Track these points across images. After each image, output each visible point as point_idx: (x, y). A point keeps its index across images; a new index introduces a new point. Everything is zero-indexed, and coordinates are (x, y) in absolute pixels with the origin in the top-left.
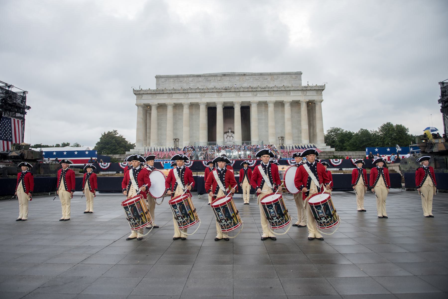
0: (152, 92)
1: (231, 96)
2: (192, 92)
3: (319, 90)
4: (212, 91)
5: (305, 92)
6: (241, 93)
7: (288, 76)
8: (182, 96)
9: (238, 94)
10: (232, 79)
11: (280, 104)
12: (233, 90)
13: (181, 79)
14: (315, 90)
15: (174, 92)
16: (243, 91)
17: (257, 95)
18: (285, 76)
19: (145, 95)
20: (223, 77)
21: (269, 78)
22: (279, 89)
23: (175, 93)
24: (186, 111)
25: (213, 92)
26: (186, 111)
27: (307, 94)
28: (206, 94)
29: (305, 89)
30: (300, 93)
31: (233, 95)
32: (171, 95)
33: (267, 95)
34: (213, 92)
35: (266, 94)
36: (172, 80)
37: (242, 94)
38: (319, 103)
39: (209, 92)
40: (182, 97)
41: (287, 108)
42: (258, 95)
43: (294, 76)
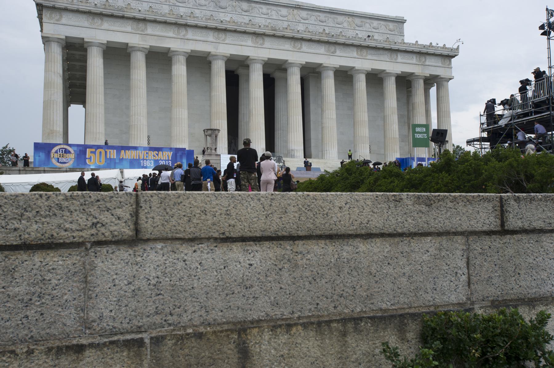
0: (93, 9)
2: (196, 27)
5: (423, 59)
7: (382, 23)
8: (170, 32)
9: (298, 44)
10: (274, 12)
12: (290, 34)
14: (441, 56)
16: (310, 40)
18: (375, 23)
19: (71, 15)
22: (380, 45)
23: (155, 21)
24: (180, 70)
25: (245, 33)
26: (180, 70)
27: (427, 63)
28: (228, 34)
29: (424, 50)
30: (414, 59)
31: (288, 45)
32: (141, 25)
34: (245, 33)
35: (354, 53)
37: (305, 47)
39: (235, 31)
40: (171, 34)
41: (391, 87)
43: (391, 25)
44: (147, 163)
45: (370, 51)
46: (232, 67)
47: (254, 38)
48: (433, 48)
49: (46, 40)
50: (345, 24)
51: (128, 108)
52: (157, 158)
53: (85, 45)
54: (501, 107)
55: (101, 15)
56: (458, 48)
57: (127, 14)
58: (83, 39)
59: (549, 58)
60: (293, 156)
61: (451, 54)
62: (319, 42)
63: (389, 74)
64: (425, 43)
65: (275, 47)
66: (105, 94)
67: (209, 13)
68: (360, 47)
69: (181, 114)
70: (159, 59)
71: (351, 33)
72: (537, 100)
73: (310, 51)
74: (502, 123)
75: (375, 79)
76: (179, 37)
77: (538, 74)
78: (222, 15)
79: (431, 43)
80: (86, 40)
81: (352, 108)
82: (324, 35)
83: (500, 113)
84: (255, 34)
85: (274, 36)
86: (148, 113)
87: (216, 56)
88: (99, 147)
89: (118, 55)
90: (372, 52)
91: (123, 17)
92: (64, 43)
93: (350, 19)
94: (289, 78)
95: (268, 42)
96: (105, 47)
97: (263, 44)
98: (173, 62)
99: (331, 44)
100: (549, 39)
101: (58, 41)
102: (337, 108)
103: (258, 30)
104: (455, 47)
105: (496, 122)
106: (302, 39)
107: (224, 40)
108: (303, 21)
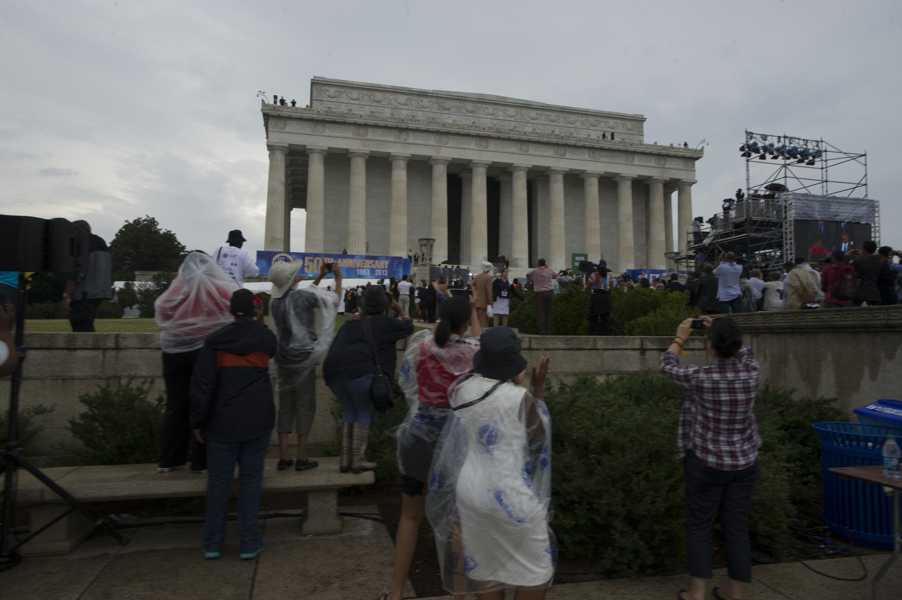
0: (316, 117)
1: (507, 150)
2: (417, 130)
4: (466, 131)
6: (531, 146)
7: (619, 121)
8: (391, 137)
10: (500, 113)
11: (609, 183)
12: (516, 137)
13: (379, 96)
14: (683, 158)
15: (373, 122)
17: (564, 154)
18: (612, 122)
19: (294, 123)
20: (478, 105)
21: (578, 120)
23: (376, 126)
24: (400, 175)
25: (468, 135)
26: (400, 175)
27: (668, 166)
28: (450, 137)
29: (664, 152)
30: (653, 162)
31: (513, 148)
32: (362, 130)
33: (587, 157)
34: (468, 135)
35: (586, 155)
36: (355, 94)
37: (532, 149)
38: (687, 188)
39: (458, 134)
40: (392, 139)
42: (568, 155)
43: (629, 125)
44: (363, 272)
45: (603, 153)
47: (478, 140)
49: (270, 147)
50: (578, 124)
51: (347, 214)
52: (373, 267)
53: (307, 152)
54: (709, 225)
55: (323, 122)
57: (349, 120)
58: (305, 146)
59: (748, 180)
60: (516, 266)
61: (695, 156)
62: (547, 144)
63: (624, 178)
64: (664, 144)
65: (500, 150)
66: (326, 201)
67: (431, 115)
68: (592, 149)
69: (400, 221)
70: (379, 165)
71: (583, 134)
72: (737, 221)
73: (537, 153)
74: (706, 241)
77: (739, 195)
78: (445, 116)
81: (583, 214)
83: (708, 230)
84: (478, 136)
85: (498, 138)
86: (367, 219)
87: (437, 161)
88: (316, 255)
89: (338, 161)
90: (607, 154)
91: (344, 123)
92: (287, 150)
93: (583, 119)
94: (514, 181)
95: (493, 145)
96: (326, 153)
97: (487, 147)
98: (393, 166)
99: (561, 146)
100: (748, 161)
101: (282, 148)
102: (566, 213)
103: (482, 133)
104: (699, 148)
105: (701, 241)
106: (529, 142)
107: (446, 143)
108: (531, 121)
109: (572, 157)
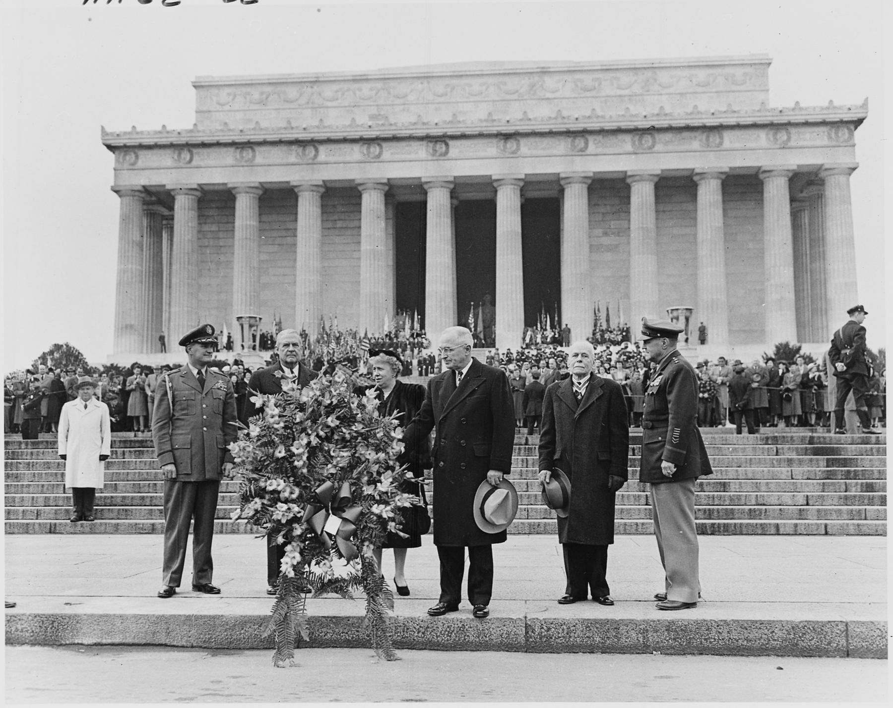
0: (175, 140)
1: (482, 154)
3: (842, 122)
5: (782, 136)
27: (792, 143)
33: (628, 147)
42: (592, 148)
46: (404, 197)
48: (803, 112)
55: (189, 146)
56: (865, 105)
58: (164, 186)
73: (535, 152)
75: (676, 189)
76: (305, 161)
79: (797, 103)
80: (168, 187)
82: (559, 120)
91: (218, 144)
101: (133, 192)
104: (860, 102)
109: (599, 150)
